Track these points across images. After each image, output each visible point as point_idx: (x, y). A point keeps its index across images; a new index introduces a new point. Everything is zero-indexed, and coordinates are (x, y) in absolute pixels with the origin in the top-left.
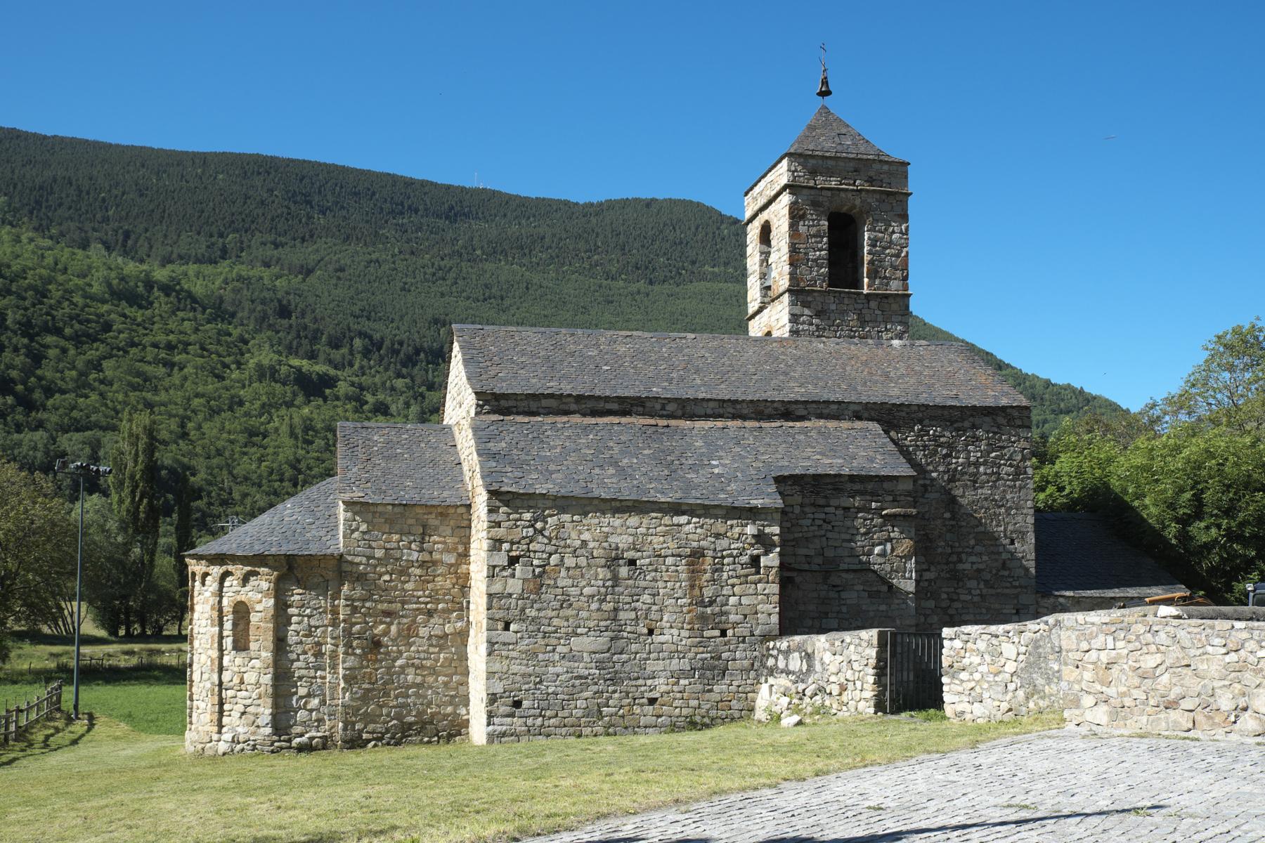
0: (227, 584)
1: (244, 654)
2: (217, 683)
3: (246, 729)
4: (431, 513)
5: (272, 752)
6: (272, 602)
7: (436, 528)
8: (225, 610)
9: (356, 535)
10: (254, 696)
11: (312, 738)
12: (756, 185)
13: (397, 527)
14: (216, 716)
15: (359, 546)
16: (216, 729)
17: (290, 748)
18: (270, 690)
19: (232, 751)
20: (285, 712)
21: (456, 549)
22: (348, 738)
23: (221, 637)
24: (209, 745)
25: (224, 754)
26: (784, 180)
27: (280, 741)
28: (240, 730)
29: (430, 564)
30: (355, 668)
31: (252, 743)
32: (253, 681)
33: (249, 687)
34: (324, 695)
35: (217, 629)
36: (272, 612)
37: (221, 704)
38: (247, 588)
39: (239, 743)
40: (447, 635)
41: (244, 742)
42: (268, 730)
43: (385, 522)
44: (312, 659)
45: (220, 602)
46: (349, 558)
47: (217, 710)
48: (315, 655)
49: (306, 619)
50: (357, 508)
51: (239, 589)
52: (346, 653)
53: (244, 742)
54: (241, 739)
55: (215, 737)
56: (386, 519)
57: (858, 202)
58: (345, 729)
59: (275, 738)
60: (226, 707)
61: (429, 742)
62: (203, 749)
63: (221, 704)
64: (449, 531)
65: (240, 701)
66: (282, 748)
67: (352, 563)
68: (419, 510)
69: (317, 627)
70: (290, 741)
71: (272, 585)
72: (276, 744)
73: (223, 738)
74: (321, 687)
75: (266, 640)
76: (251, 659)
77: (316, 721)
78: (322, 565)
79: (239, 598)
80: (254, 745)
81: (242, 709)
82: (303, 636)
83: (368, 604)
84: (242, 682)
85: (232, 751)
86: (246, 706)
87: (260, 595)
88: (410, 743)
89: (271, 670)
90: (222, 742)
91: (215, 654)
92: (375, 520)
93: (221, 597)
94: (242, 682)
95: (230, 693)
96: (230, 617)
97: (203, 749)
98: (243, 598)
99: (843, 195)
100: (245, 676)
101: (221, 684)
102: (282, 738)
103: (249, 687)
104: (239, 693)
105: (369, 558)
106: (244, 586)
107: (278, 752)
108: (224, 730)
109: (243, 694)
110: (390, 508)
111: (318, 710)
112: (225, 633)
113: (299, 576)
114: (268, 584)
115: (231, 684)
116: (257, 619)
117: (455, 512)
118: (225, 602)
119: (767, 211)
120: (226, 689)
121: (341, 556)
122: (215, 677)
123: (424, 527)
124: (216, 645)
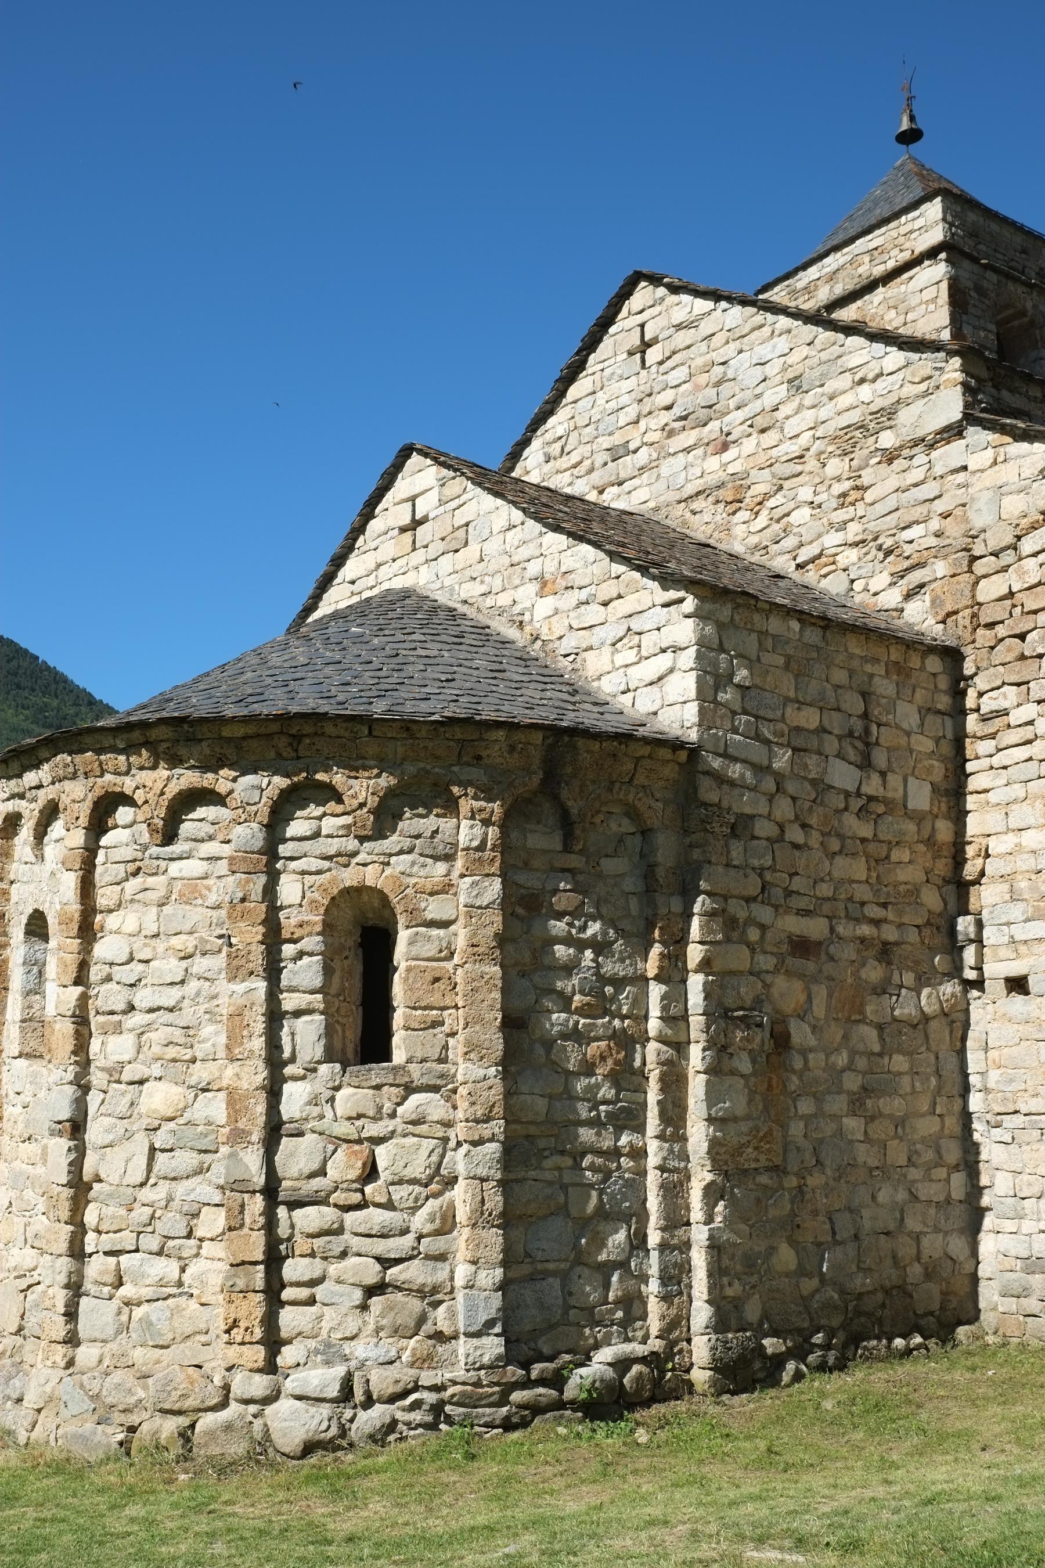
0: (297, 827)
1: (376, 1072)
2: (260, 1180)
3: (388, 1347)
4: (876, 660)
5: (508, 1426)
6: (494, 888)
7: (892, 708)
8: (289, 920)
9: (726, 696)
10: (419, 1221)
11: (622, 1365)
12: (805, 267)
13: (813, 688)
14: (254, 1307)
15: (735, 731)
16: (258, 1354)
17: (560, 1405)
18: (495, 1201)
19: (343, 1432)
20: (532, 1278)
21: (929, 770)
22: (733, 1354)
23: (275, 1017)
24: (207, 1421)
25: (309, 1448)
26: (936, 235)
27: (526, 1384)
28: (360, 1350)
29: (881, 809)
30: (735, 1119)
31: (430, 1397)
32: (418, 1169)
33: (399, 1193)
34: (643, 1216)
35: (261, 986)
36: (495, 921)
37: (274, 1259)
38: (392, 843)
39: (369, 1402)
40: (926, 1018)
41: (392, 1399)
42: (493, 1346)
43: (787, 667)
44: (606, 1092)
45: (270, 892)
46: (716, 763)
47: (259, 1281)
48: (615, 1078)
49: (589, 954)
50: (725, 612)
51: (352, 844)
52: (713, 1071)
53: (392, 1399)
54: (381, 1381)
55: (260, 1385)
56: (789, 659)
57: (1029, 305)
58: (720, 1325)
59: (515, 1372)
60: (293, 1269)
61: (908, 1352)
62: (186, 1435)
63: (274, 1259)
64: (914, 720)
65: (357, 1243)
66: (536, 1409)
67: (720, 779)
68: (855, 646)
69: (619, 983)
70: (557, 1381)
71: (493, 832)
72: (517, 1396)
73: (290, 1385)
74: (636, 1185)
75: (480, 1020)
76: (410, 1089)
77: (617, 1302)
78: (640, 779)
79: (349, 877)
80: (437, 1409)
81: (371, 1273)
82: (581, 1012)
83: (764, 913)
84: (371, 1173)
85: (343, 1432)
86: (386, 1263)
87: (441, 868)
88: (870, 1358)
89: (497, 1127)
90: (285, 1405)
91: (255, 1074)
92: (767, 658)
93: (273, 877)
94: (371, 1173)
95: (309, 1218)
96: (312, 942)
97: (186, 1435)
98: (371, 876)
99: (1011, 286)
100: (382, 1153)
101: (271, 1191)
102: (535, 1372)
103: (399, 1193)
104: (350, 1218)
105: (761, 769)
106: (379, 833)
107: (524, 1424)
108: (288, 1355)
109: (376, 1218)
110: (795, 625)
111: (623, 1265)
112: (289, 1002)
113: (574, 807)
114: (478, 830)
115: (317, 1183)
116: (430, 950)
117: (923, 668)
118: (289, 890)
119: (859, 303)
120: (294, 1205)
121: (694, 752)
122: (252, 1161)
123: (865, 695)
124: (258, 1044)
